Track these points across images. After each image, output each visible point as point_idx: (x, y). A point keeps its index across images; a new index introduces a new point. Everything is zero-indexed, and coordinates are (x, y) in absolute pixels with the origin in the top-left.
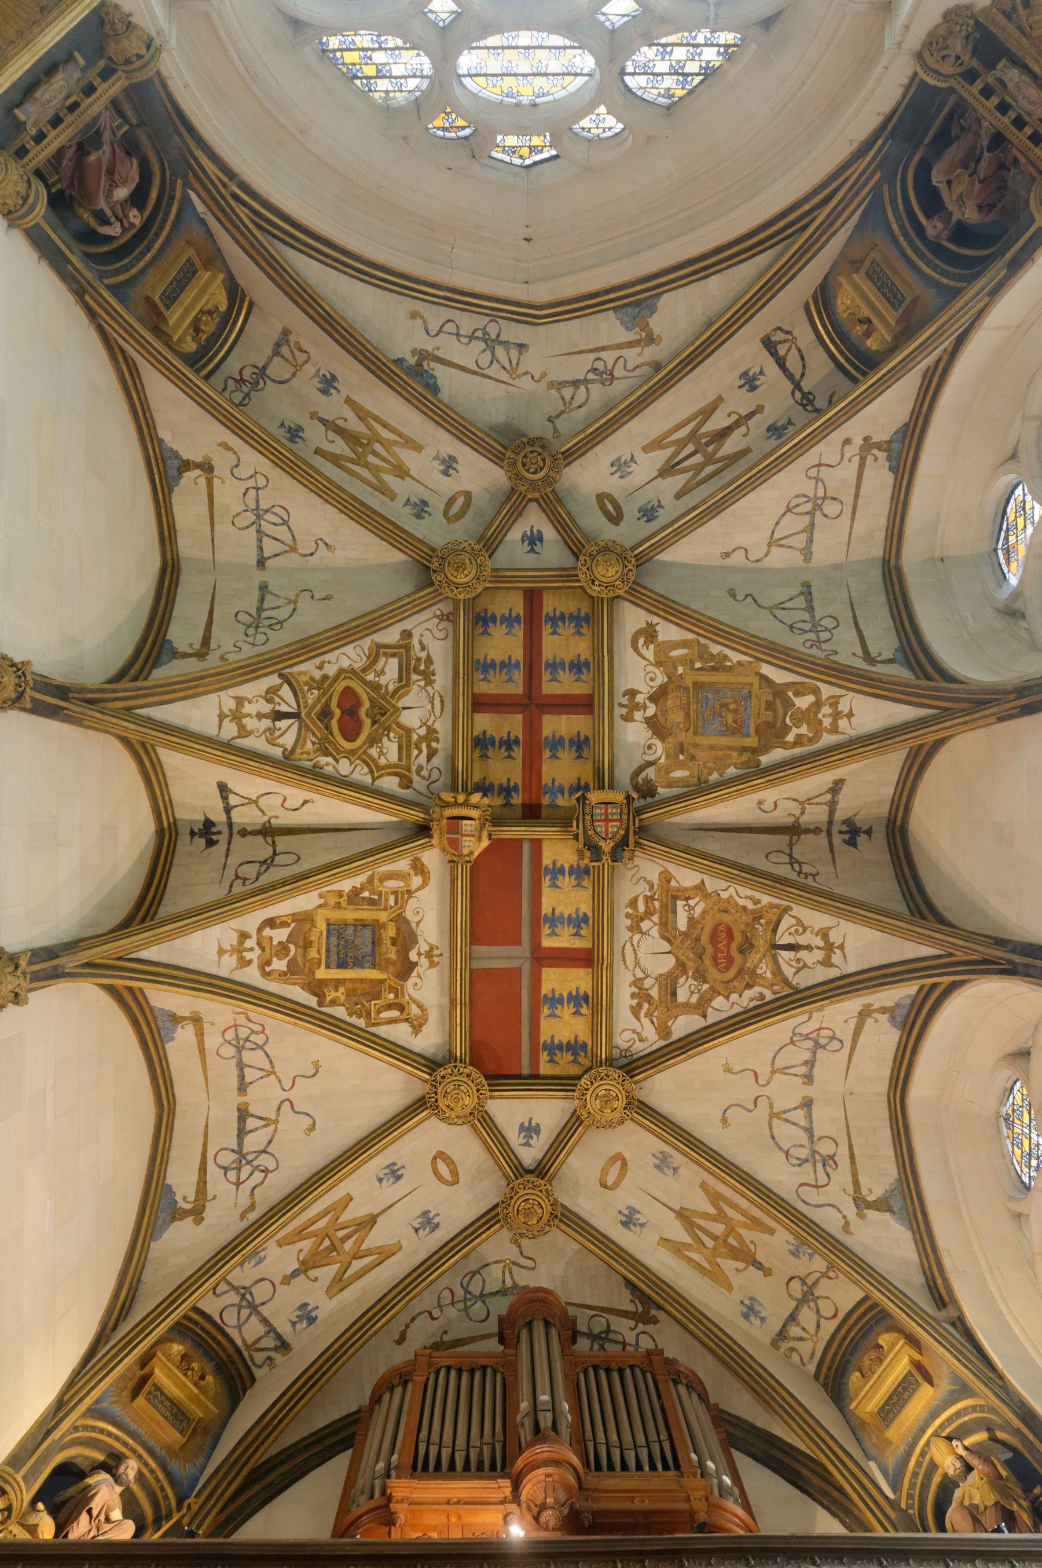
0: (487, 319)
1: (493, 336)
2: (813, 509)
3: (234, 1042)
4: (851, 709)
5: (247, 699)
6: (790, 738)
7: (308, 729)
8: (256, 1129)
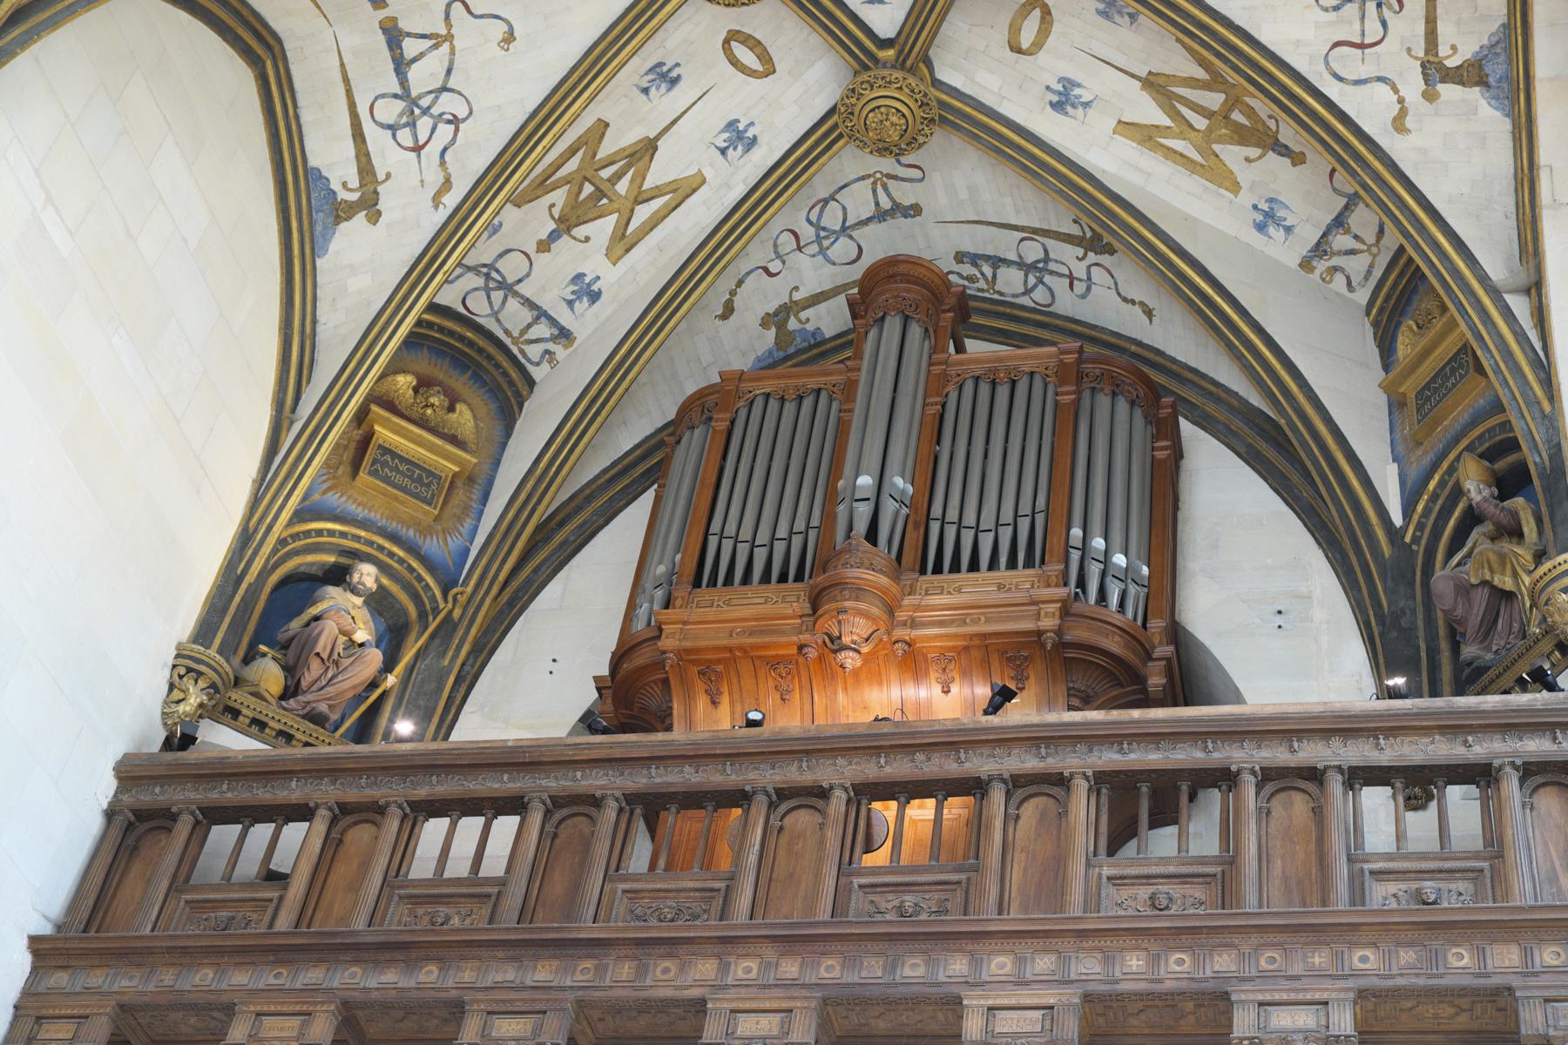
8: (422, 55)
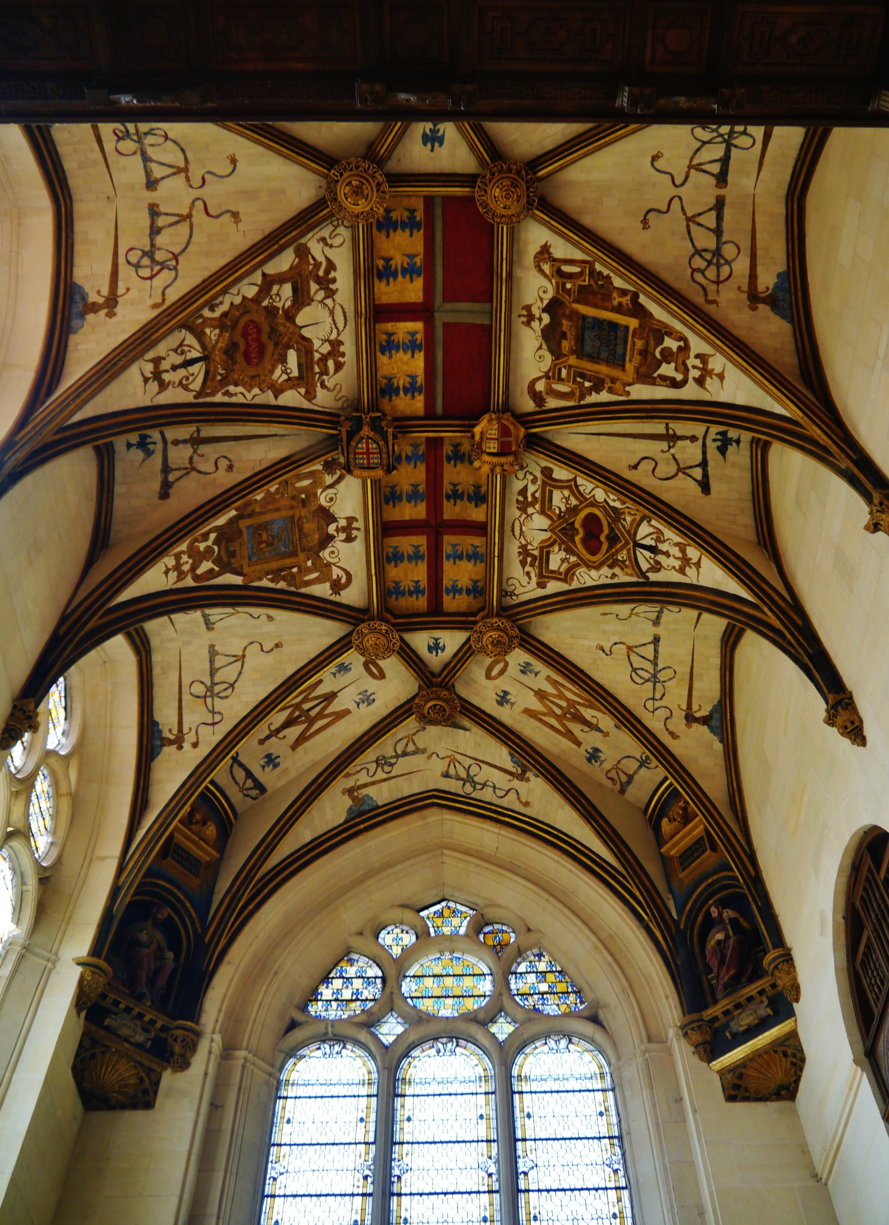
0: (473, 795)
1: (468, 784)
2: (213, 687)
3: (722, 261)
4: (167, 576)
5: (676, 570)
6: (213, 536)
7: (628, 532)
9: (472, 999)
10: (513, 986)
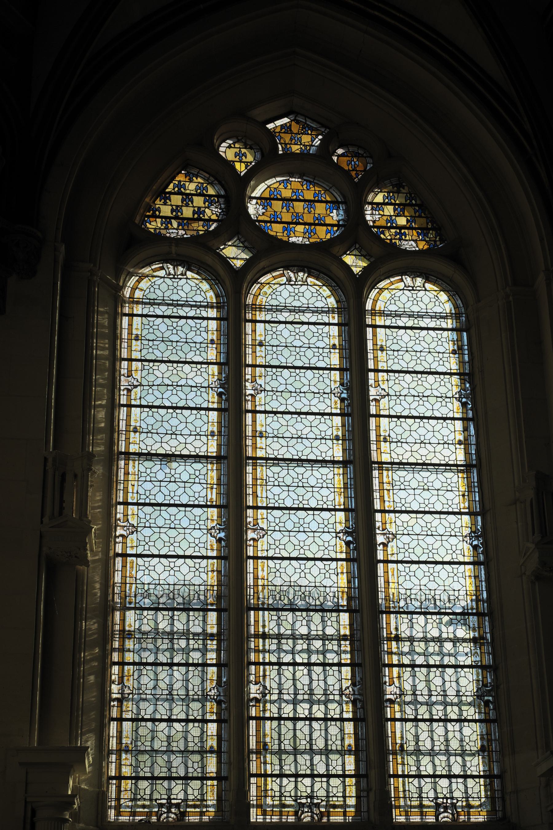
9: (325, 228)
10: (368, 218)
